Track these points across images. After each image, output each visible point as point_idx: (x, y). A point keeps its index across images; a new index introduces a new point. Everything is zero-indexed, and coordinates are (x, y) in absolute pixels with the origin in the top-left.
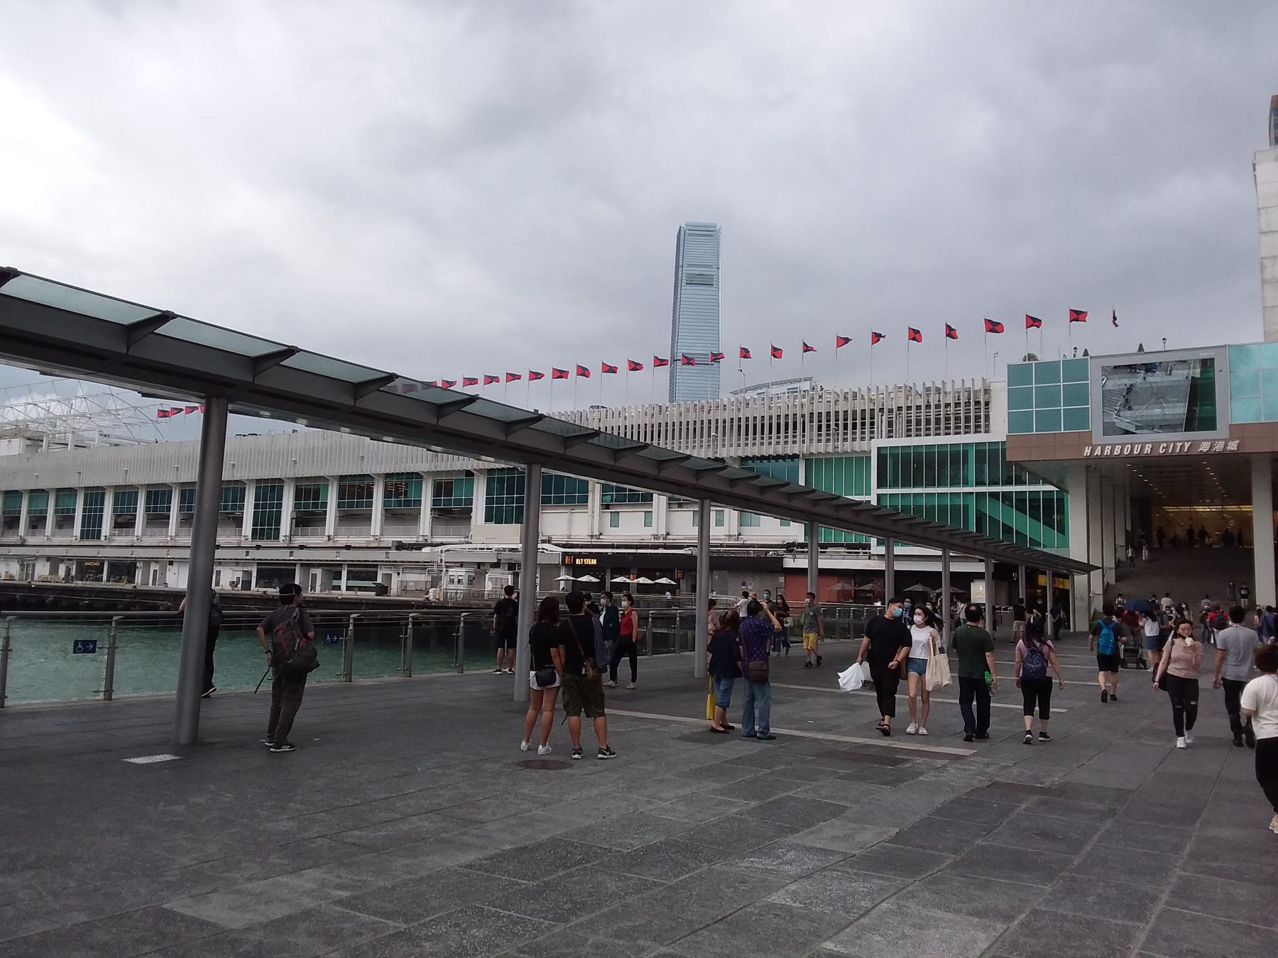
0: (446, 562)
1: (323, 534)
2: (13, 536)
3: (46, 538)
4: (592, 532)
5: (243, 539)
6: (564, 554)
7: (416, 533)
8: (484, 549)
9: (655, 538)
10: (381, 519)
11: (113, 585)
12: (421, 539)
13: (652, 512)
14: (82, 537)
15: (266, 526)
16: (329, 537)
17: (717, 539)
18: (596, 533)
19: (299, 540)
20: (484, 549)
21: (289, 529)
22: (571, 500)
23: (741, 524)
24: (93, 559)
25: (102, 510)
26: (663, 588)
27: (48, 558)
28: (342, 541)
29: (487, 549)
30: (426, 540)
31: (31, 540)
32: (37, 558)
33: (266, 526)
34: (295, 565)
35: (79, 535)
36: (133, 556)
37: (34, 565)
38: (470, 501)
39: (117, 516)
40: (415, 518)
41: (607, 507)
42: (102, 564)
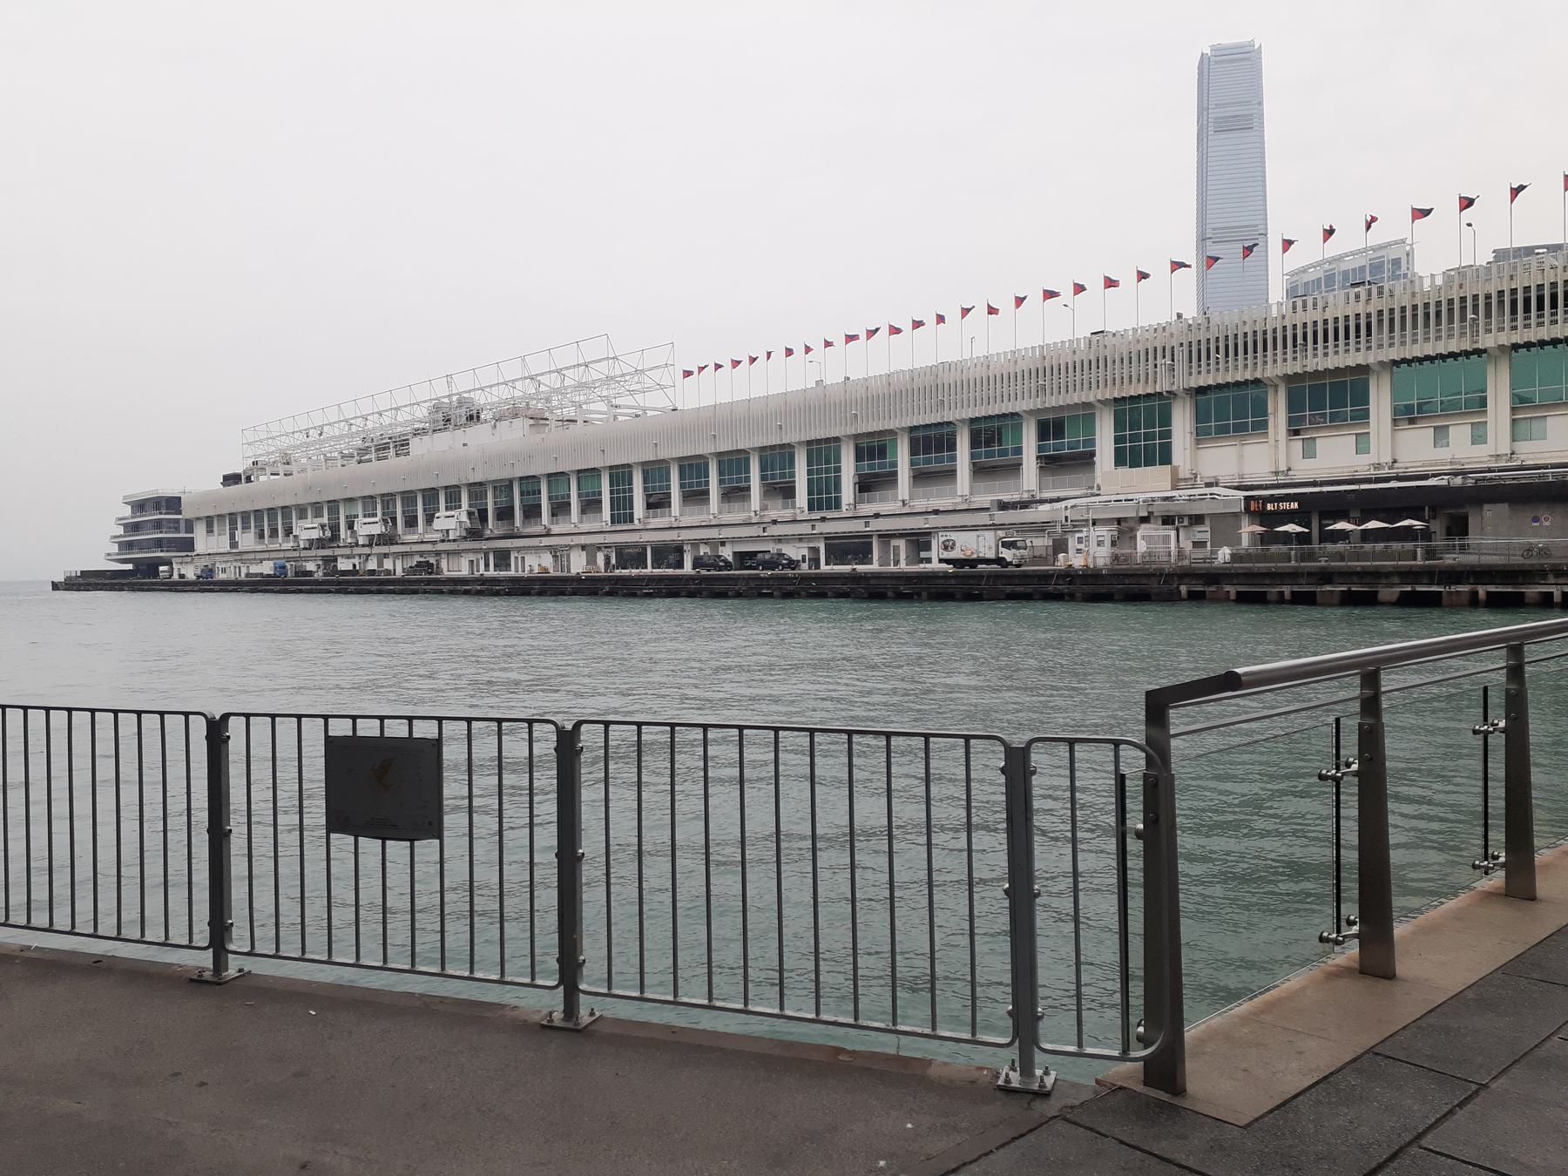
0: (1071, 521)
1: (895, 499)
2: (536, 524)
3: (573, 526)
5: (798, 511)
6: (1246, 498)
7: (1018, 489)
8: (1121, 501)
9: (1375, 468)
10: (970, 475)
11: (657, 571)
12: (1026, 496)
13: (1369, 433)
14: (613, 522)
15: (824, 497)
16: (903, 501)
17: (1476, 462)
18: (1283, 468)
19: (867, 509)
20: (1121, 501)
21: (853, 496)
22: (1240, 429)
23: (1514, 439)
24: (634, 545)
25: (631, 490)
26: (1409, 533)
27: (583, 547)
28: (920, 504)
29: (1125, 500)
30: (1033, 496)
31: (556, 529)
32: (571, 547)
33: (824, 497)
34: (871, 536)
35: (609, 519)
36: (680, 539)
37: (568, 556)
38: (1092, 442)
39: (648, 496)
40: (1016, 468)
41: (1296, 433)
42: (645, 550)
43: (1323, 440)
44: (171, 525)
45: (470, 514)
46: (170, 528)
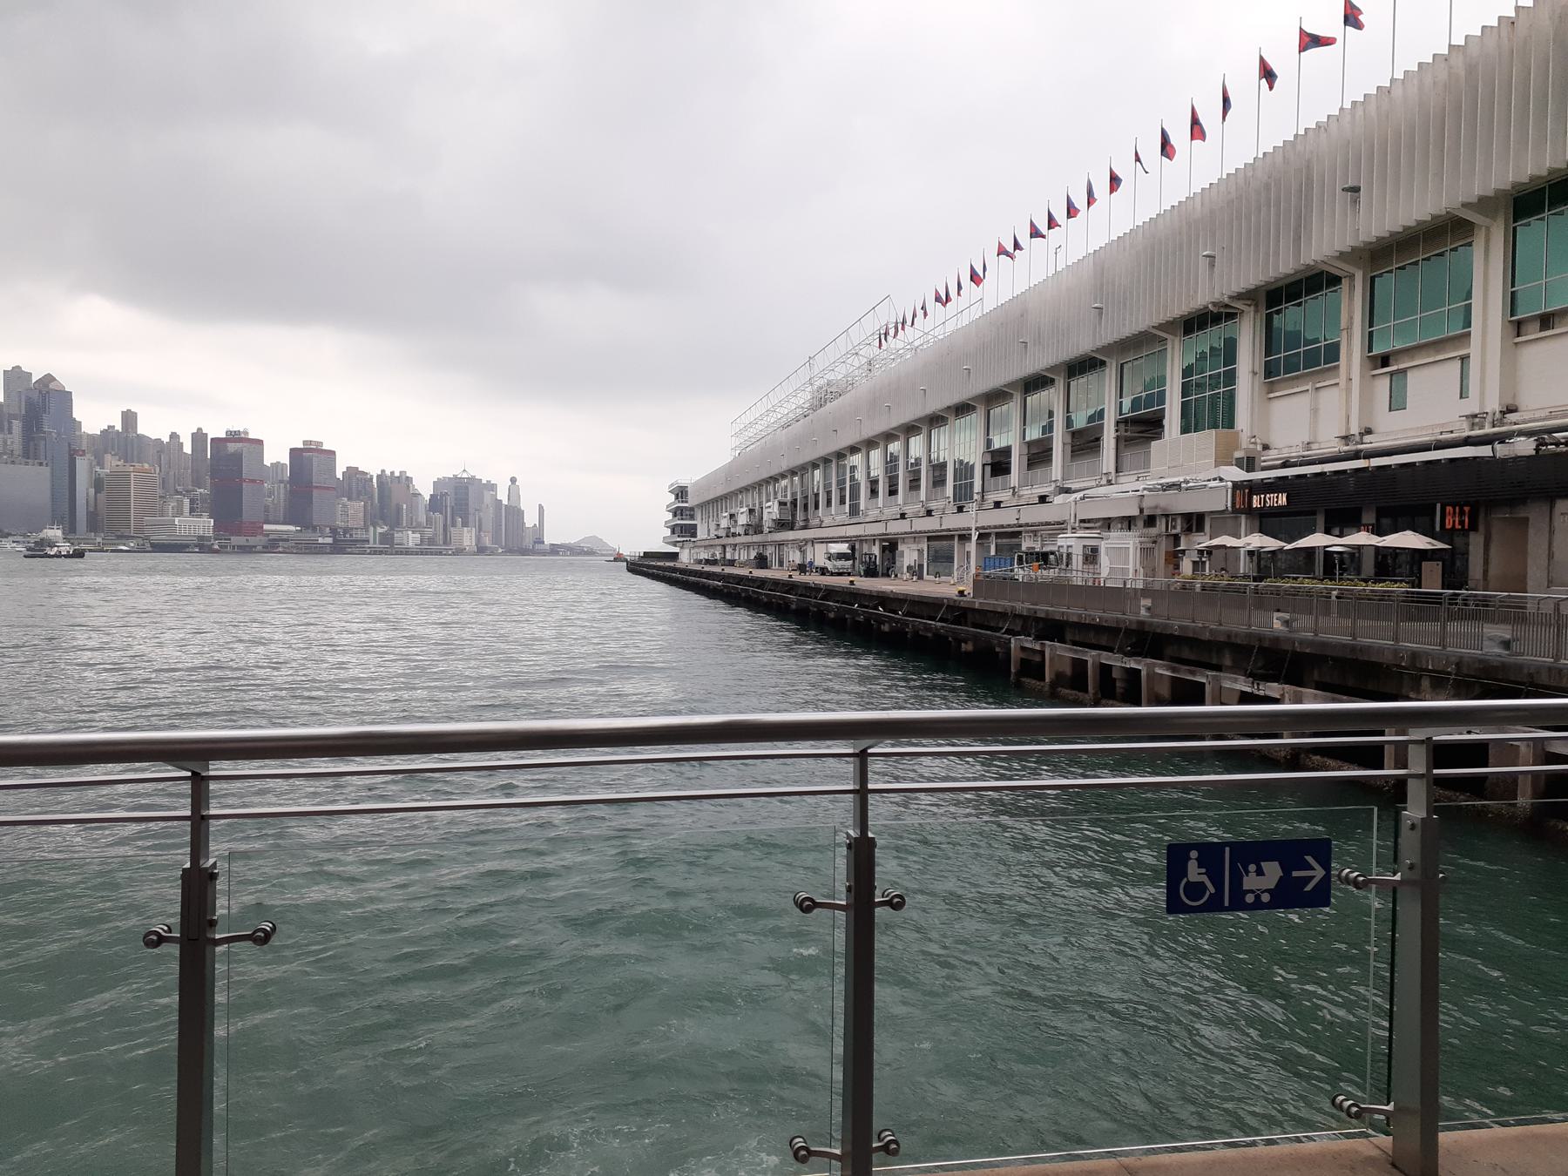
4: (1348, 429)
18: (1355, 430)
41: (1385, 361)
43: (1415, 370)
44: (688, 513)
45: (782, 504)
46: (687, 515)
